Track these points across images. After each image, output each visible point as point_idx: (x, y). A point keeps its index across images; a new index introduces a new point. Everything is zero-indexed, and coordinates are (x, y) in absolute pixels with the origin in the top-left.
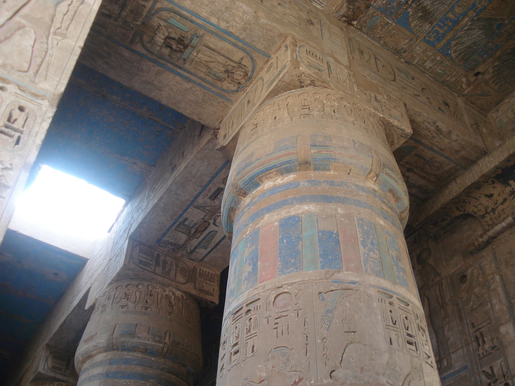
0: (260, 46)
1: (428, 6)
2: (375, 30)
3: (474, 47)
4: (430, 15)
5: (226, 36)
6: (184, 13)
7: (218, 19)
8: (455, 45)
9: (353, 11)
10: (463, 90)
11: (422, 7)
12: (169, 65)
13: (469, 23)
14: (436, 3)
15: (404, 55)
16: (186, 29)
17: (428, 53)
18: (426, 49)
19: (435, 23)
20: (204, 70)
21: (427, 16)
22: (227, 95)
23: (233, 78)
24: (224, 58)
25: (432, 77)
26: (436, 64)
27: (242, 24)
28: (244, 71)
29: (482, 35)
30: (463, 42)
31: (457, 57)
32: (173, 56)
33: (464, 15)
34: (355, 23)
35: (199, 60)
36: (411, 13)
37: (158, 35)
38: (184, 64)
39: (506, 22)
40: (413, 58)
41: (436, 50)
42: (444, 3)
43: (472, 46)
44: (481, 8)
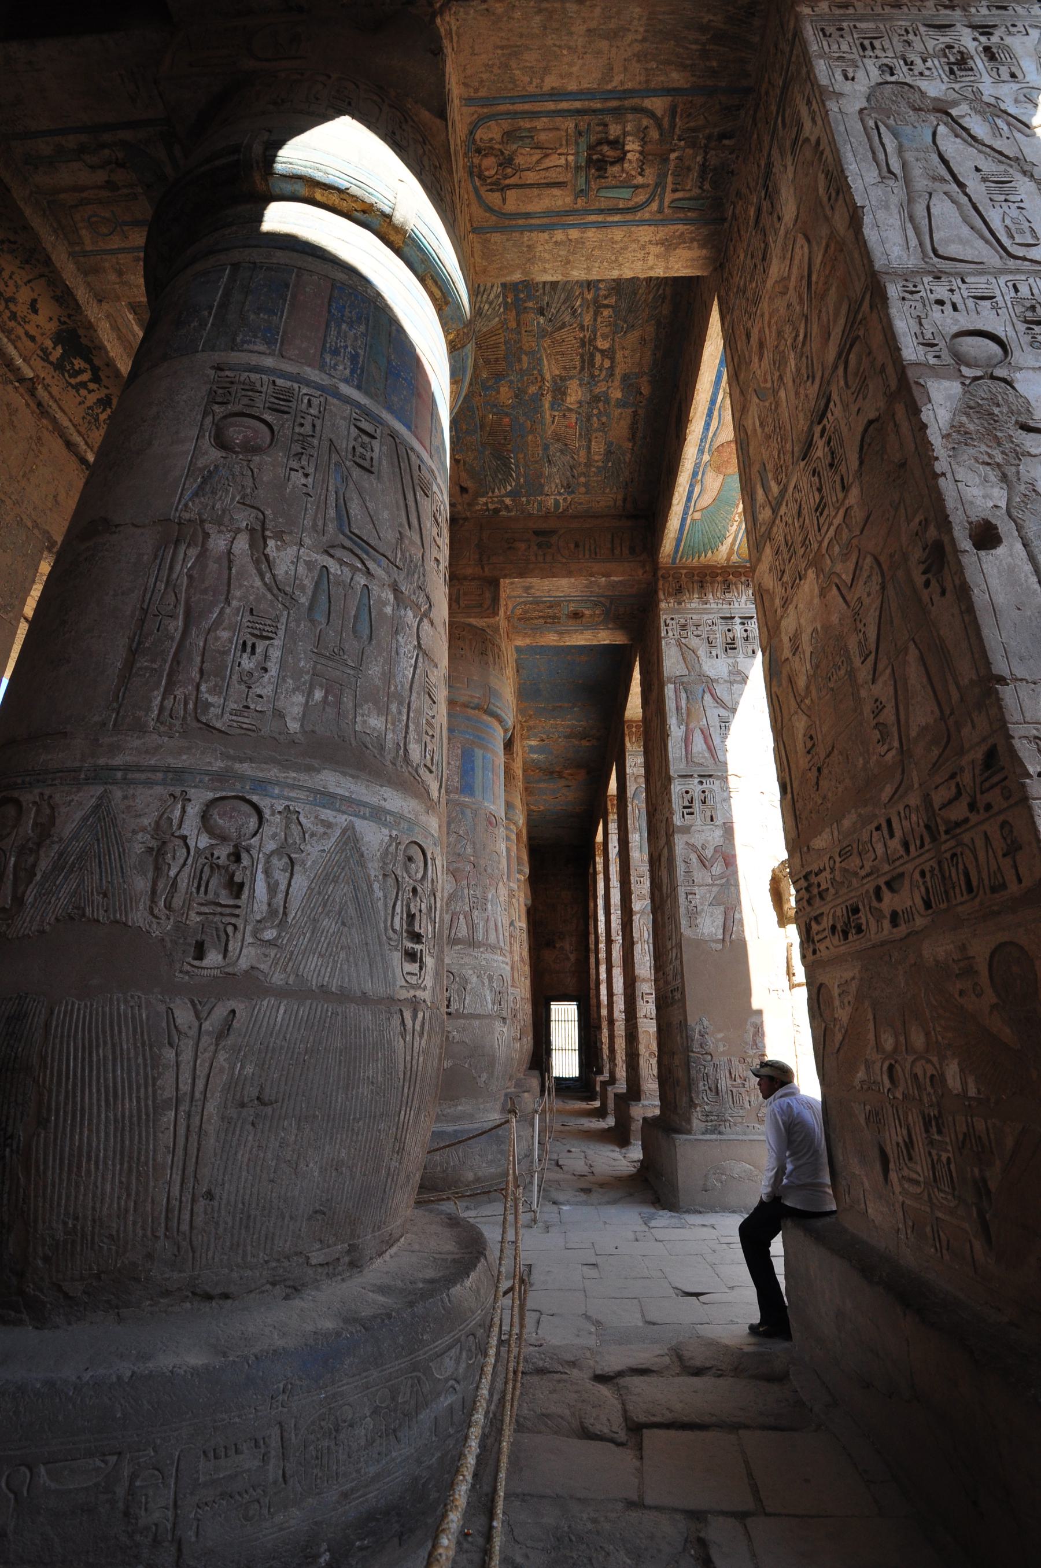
0: (496, 237)
5: (546, 221)
6: (617, 218)
7: (571, 240)
12: (599, 106)
16: (603, 193)
20: (543, 137)
22: (480, 110)
23: (496, 156)
24: (528, 182)
27: (538, 254)
28: (489, 181)
32: (600, 128)
35: (559, 151)
37: (637, 155)
38: (576, 126)
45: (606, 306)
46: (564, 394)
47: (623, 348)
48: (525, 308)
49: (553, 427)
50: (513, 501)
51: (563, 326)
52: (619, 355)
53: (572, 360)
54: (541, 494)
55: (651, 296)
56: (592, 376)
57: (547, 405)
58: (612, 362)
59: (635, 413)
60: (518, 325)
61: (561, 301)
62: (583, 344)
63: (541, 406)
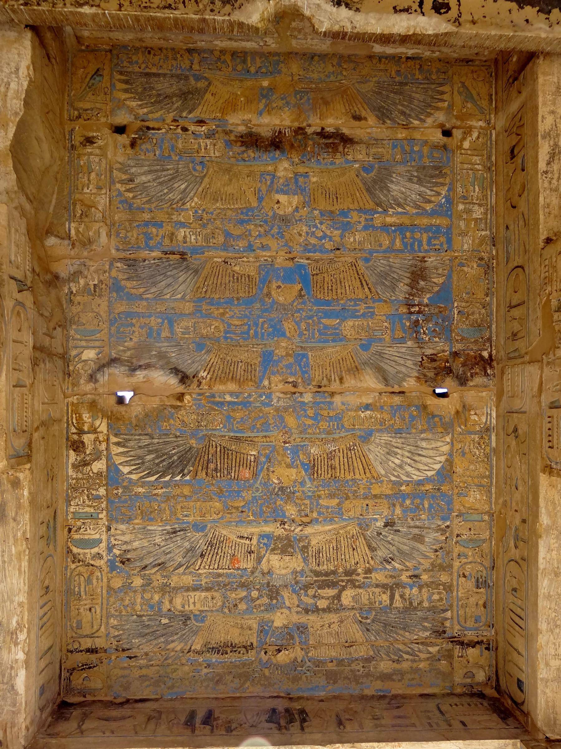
1: (406, 282)
2: (479, 320)
3: (416, 174)
4: (415, 269)
8: (430, 202)
9: (472, 368)
10: (481, 131)
11: (412, 288)
13: (391, 211)
14: (395, 276)
15: (485, 256)
17: (463, 228)
18: (460, 235)
19: (421, 254)
21: (419, 273)
25: (492, 191)
26: (470, 203)
29: (394, 180)
30: (419, 195)
31: (443, 184)
33: (385, 227)
34: (485, 354)
36: (428, 296)
39: (357, 166)
40: (482, 240)
41: (451, 221)
42: (389, 266)
43: (415, 179)
44: (363, 216)
45: (392, 597)
46: (284, 551)
47: (342, 622)
48: (394, 505)
49: (233, 537)
50: (99, 474)
51: (372, 549)
52: (333, 617)
53: (329, 560)
54: (111, 519)
55: (401, 647)
56: (306, 587)
57: (268, 529)
58: (324, 610)
59: (249, 647)
60: (375, 496)
61: (401, 546)
62: (348, 573)
63: (266, 521)
